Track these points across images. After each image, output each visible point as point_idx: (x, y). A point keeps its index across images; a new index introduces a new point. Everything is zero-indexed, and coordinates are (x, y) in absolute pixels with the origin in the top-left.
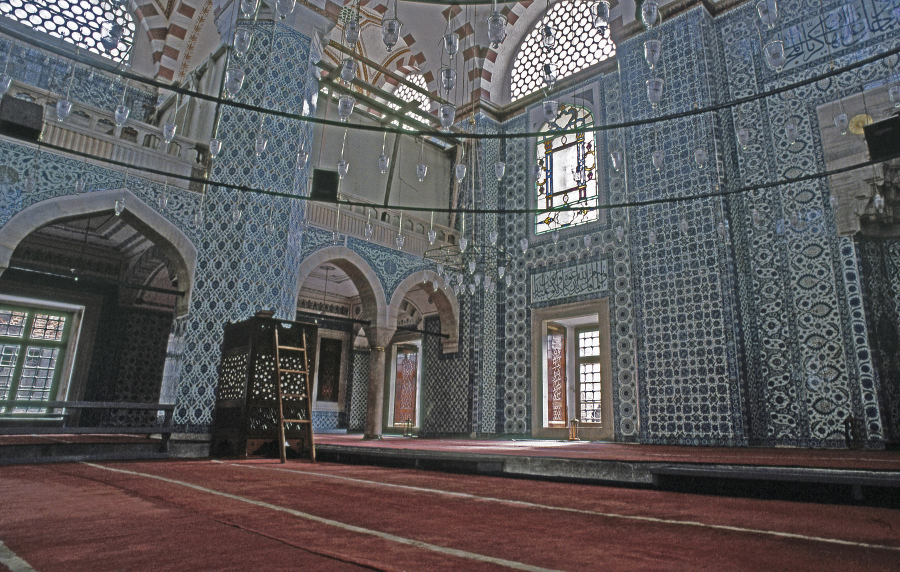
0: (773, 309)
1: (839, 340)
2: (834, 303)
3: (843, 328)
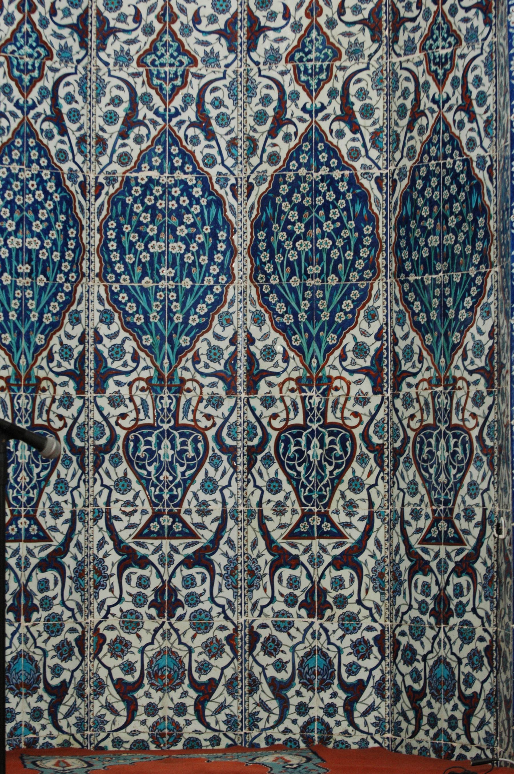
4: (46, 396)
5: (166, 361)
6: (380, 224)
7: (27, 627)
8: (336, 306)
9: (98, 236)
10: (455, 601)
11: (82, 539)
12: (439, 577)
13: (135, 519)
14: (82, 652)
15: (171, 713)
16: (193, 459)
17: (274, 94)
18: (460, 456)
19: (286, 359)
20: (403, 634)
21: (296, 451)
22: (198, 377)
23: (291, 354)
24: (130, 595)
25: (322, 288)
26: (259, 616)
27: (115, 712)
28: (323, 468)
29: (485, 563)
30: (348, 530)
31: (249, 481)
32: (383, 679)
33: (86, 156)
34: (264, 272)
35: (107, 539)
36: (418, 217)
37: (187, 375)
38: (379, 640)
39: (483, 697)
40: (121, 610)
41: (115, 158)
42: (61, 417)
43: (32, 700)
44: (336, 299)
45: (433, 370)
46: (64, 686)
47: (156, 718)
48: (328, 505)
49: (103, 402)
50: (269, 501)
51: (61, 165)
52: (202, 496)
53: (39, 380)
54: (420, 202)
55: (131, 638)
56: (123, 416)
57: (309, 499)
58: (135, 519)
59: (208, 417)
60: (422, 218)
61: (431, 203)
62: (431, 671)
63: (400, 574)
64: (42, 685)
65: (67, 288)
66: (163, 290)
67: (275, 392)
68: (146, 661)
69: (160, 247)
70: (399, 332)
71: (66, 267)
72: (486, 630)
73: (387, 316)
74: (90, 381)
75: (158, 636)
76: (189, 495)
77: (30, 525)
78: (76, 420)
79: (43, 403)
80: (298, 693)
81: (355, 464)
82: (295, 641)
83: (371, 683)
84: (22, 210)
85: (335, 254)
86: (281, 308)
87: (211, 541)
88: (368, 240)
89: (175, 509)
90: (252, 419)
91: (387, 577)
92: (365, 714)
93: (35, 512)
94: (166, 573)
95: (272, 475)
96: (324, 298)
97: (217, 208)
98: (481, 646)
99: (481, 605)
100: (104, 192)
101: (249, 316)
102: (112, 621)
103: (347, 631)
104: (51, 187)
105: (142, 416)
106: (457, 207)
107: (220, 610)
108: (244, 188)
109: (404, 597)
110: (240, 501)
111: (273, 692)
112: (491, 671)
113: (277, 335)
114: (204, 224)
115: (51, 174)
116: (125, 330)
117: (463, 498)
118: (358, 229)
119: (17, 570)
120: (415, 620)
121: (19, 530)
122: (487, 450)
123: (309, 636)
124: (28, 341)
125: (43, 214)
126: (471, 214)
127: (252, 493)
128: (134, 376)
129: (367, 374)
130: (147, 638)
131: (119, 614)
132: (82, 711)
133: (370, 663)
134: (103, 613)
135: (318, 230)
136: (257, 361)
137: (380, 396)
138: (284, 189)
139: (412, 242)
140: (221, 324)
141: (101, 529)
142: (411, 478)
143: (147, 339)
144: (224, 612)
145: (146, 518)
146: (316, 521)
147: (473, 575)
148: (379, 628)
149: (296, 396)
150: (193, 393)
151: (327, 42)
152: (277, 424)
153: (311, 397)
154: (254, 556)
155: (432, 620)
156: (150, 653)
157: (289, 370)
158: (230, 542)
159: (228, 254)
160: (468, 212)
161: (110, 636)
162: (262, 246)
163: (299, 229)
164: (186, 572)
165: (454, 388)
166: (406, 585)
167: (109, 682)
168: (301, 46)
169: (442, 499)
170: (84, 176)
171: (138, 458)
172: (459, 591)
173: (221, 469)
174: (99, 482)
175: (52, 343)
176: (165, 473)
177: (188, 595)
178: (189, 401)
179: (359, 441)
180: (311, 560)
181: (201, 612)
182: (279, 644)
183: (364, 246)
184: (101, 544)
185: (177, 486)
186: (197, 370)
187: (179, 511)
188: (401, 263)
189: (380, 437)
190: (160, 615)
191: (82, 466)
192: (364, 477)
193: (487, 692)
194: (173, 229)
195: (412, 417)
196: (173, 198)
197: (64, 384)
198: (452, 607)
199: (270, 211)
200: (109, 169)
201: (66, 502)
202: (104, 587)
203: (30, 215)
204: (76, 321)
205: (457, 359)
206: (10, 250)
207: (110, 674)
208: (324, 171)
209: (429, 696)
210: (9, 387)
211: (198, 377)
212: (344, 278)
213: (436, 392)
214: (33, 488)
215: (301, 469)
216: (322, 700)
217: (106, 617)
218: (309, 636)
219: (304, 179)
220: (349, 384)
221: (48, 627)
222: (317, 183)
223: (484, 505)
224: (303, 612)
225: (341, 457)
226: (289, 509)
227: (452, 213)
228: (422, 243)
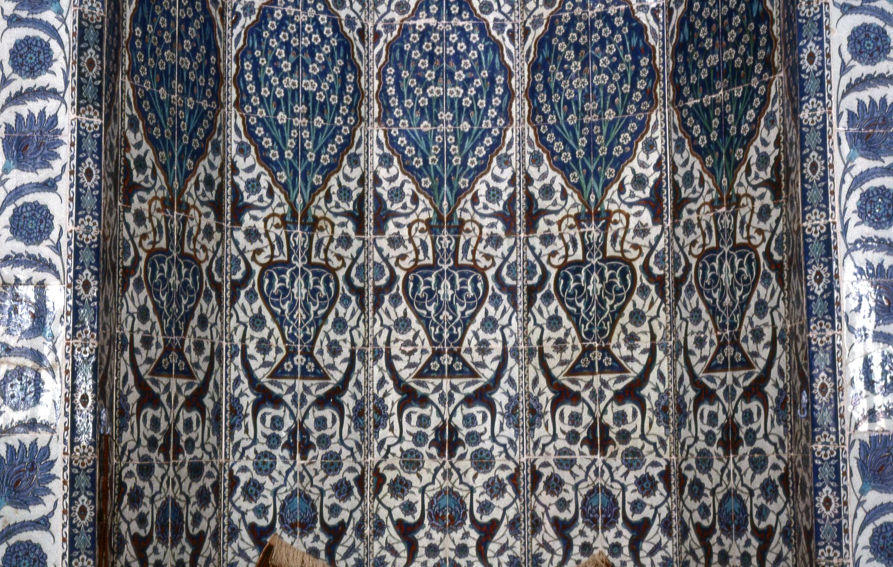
4: (325, 235)
5: (445, 202)
6: (657, 55)
7: (303, 465)
8: (613, 141)
9: (376, 83)
10: (744, 430)
11: (361, 378)
12: (727, 405)
13: (415, 358)
15: (452, 555)
16: (473, 298)
18: (746, 275)
19: (564, 196)
20: (689, 468)
21: (576, 287)
22: (477, 218)
23: (569, 191)
24: (410, 434)
25: (600, 123)
26: (541, 454)
28: (603, 303)
29: (776, 385)
30: (630, 364)
31: (529, 320)
32: (669, 517)
33: (363, 5)
34: (542, 113)
35: (387, 378)
36: (695, 40)
37: (466, 216)
38: (665, 476)
39: (778, 530)
40: (401, 450)
41: (393, 7)
42: (340, 257)
43: (309, 540)
44: (614, 134)
45: (714, 193)
46: (343, 526)
47: (437, 559)
48: (609, 339)
49: (383, 243)
50: (549, 339)
51: (339, 12)
52: (482, 335)
53: (316, 219)
54: (698, 24)
55: (412, 478)
56: (403, 257)
57: (589, 334)
58: (415, 358)
59: (488, 257)
60: (700, 40)
61: (710, 22)
62: (720, 505)
63: (685, 406)
64: (318, 525)
65: (346, 130)
66: (442, 134)
67: (554, 230)
68: (427, 501)
69: (438, 92)
71: (343, 110)
72: (779, 457)
73: (665, 146)
74: (369, 222)
75: (439, 476)
76: (469, 335)
77: (306, 363)
78: (354, 260)
79: (320, 242)
80: (582, 533)
81: (635, 297)
82: (578, 480)
83: (657, 521)
84: (298, 53)
86: (558, 146)
87: (491, 380)
88: (644, 73)
89: (456, 349)
90: (531, 257)
91: (671, 411)
92: (652, 553)
93: (312, 349)
94: (446, 412)
95: (552, 312)
96: (601, 133)
97: (494, 53)
98: (775, 475)
99: (774, 431)
100: (382, 40)
101: (527, 157)
102: (391, 460)
103: (630, 466)
104: (328, 32)
105: (421, 256)
106: (737, 20)
107: (502, 449)
108: (521, 33)
109: (690, 429)
110: (521, 340)
111: (557, 532)
112: (788, 501)
113: (555, 174)
114: (481, 70)
115: (328, 19)
116: (405, 174)
117: (750, 319)
118: (636, 62)
119: (293, 408)
120: (703, 453)
121: (295, 367)
122: (777, 266)
123: (591, 473)
124: (305, 180)
125: (320, 57)
126: (752, 24)
127: (533, 332)
128: (413, 217)
129: (645, 206)
131: (399, 454)
132: (361, 552)
133: (656, 499)
134: (383, 452)
135: (595, 67)
136: (536, 201)
137: (660, 227)
138: (560, 30)
139: (690, 66)
140: (500, 166)
141: (381, 369)
142: (694, 306)
143: (426, 183)
144: (506, 451)
145: (426, 357)
146: (597, 356)
147: (764, 399)
148: (664, 463)
149: (576, 232)
150: (472, 234)
152: (557, 261)
153: (589, 233)
154: (535, 394)
155: (720, 451)
156: (431, 493)
157: (567, 207)
158: (511, 381)
159: (506, 98)
160: (748, 22)
161: (390, 475)
162: (539, 87)
164: (467, 411)
165: (738, 205)
166: (691, 416)
167: (390, 523)
169: (728, 323)
170: (363, 25)
171: (418, 298)
172: (748, 417)
173: (501, 308)
174: (378, 322)
175: (329, 184)
176: (445, 313)
177: (469, 435)
178: (468, 242)
179: (639, 273)
180: (593, 395)
181: (481, 451)
183: (641, 78)
184: (382, 382)
185: (457, 326)
186: (475, 211)
187: (459, 350)
188: (678, 90)
189: (661, 269)
190: (441, 453)
191: (362, 305)
192: (646, 309)
193: (783, 525)
194: (451, 74)
195: (693, 243)
196: (451, 44)
197: (343, 225)
198: (742, 435)
199: (546, 53)
200: (388, 17)
201: (345, 341)
202: (384, 427)
203: (307, 58)
204: (354, 161)
206: (286, 91)
207: (390, 514)
209: (718, 532)
211: (477, 218)
212: (621, 112)
213: (718, 214)
214: (310, 325)
215: (581, 305)
216: (606, 540)
217: (386, 457)
218: (591, 473)
219: (580, 19)
220: (628, 216)
221: (326, 466)
222: (593, 21)
223: (773, 323)
224: (586, 449)
225: (621, 291)
226: (570, 346)
227: (731, 27)
228: (700, 64)
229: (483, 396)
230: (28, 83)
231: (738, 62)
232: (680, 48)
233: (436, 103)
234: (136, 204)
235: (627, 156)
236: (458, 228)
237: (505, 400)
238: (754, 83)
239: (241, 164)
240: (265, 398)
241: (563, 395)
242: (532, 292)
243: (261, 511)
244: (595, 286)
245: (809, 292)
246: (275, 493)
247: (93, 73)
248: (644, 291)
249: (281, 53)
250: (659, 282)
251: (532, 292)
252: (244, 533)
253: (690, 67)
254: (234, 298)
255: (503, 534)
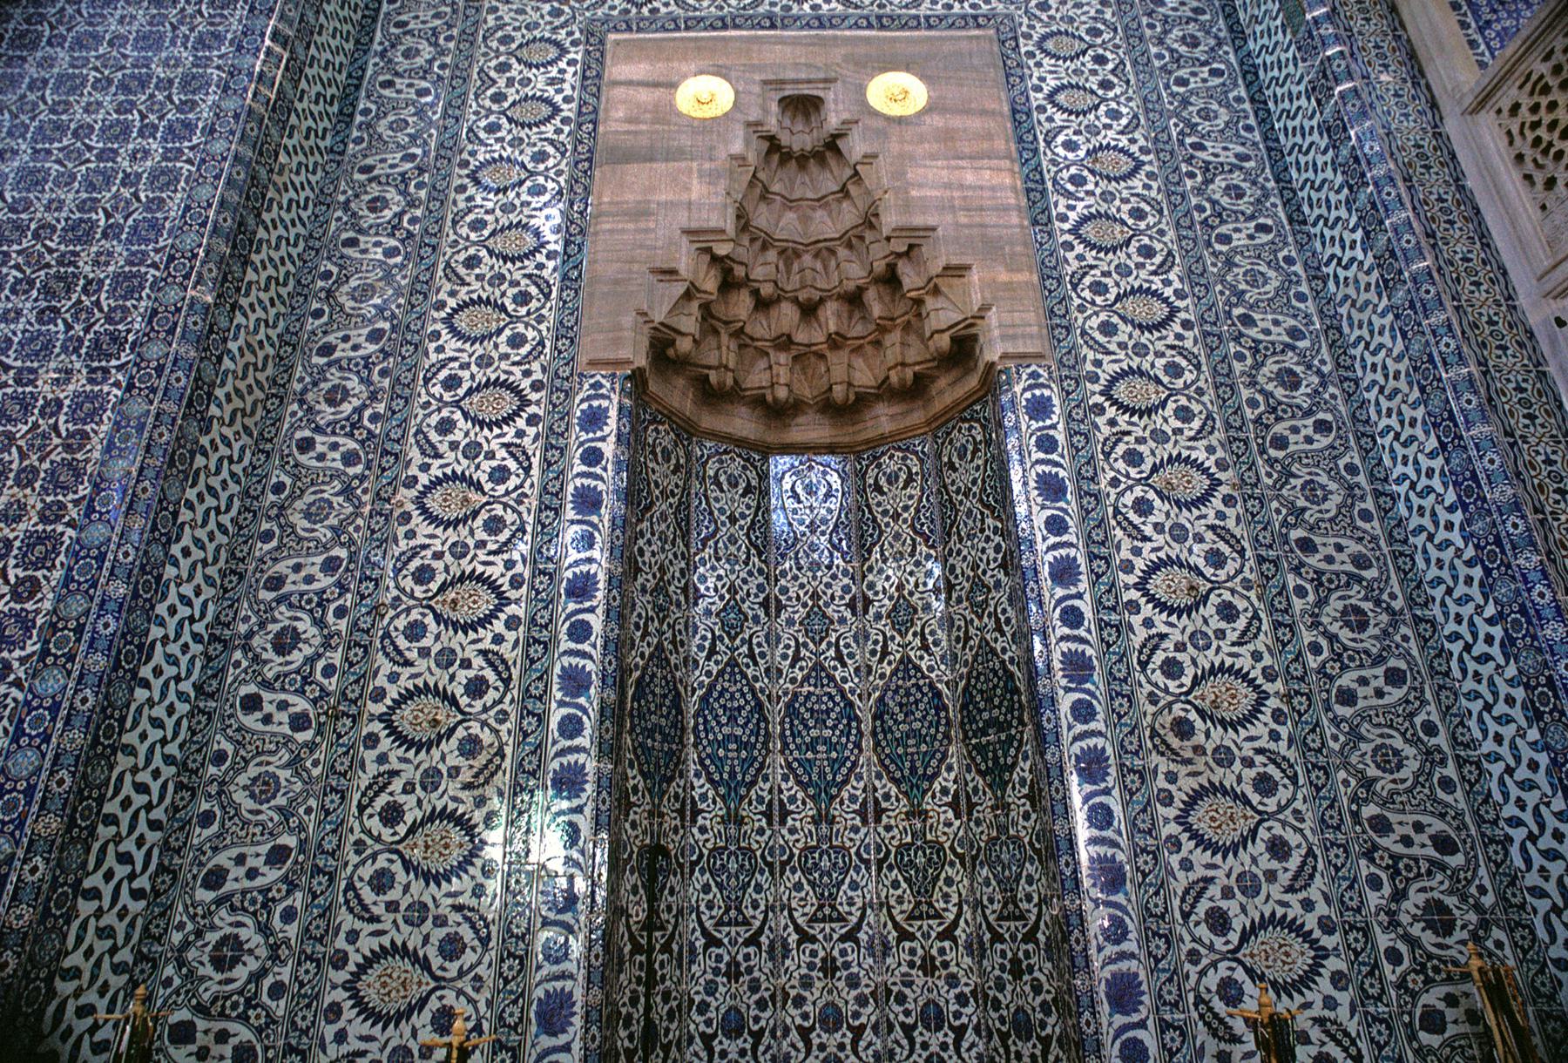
0: (309, 579)
1: (503, 717)
2: (516, 582)
3: (525, 671)
10: (1025, 963)
13: (807, 910)
14: (774, 1005)
17: (881, 638)
27: (798, 1050)
38: (974, 993)
46: (762, 1030)
49: (784, 832)
52: (850, 893)
55: (807, 994)
58: (807, 910)
61: (981, 692)
65: (760, 759)
67: (893, 822)
70: (969, 778)
71: (759, 746)
85: (924, 731)
86: (892, 768)
88: (943, 721)
92: (969, 1050)
98: (1049, 998)
102: (794, 982)
106: (999, 692)
118: (937, 714)
120: (999, 978)
125: (744, 713)
130: (817, 994)
133: (969, 1010)
151: (909, 605)
152: (895, 843)
156: (820, 1004)
161: (793, 993)
163: (901, 717)
168: (895, 608)
182: (906, 997)
184: (786, 927)
191: (772, 873)
204: (766, 779)
205: (1009, 790)
208: (913, 681)
210: (723, 822)
229: (851, 936)
230: (568, 743)
231: (1002, 718)
232: (964, 707)
233: (815, 740)
234: (632, 817)
235: (936, 775)
236: (831, 821)
237: (866, 938)
238: (1013, 731)
239: (696, 783)
240: (712, 941)
241: (904, 936)
242: (880, 863)
243: (708, 1023)
244: (920, 860)
245: (1062, 873)
246: (717, 1009)
247: (607, 737)
248: (952, 864)
249: (721, 712)
250: (961, 857)
251: (880, 863)
252: (698, 1040)
253: (972, 721)
254: (692, 872)
255: (868, 1035)
